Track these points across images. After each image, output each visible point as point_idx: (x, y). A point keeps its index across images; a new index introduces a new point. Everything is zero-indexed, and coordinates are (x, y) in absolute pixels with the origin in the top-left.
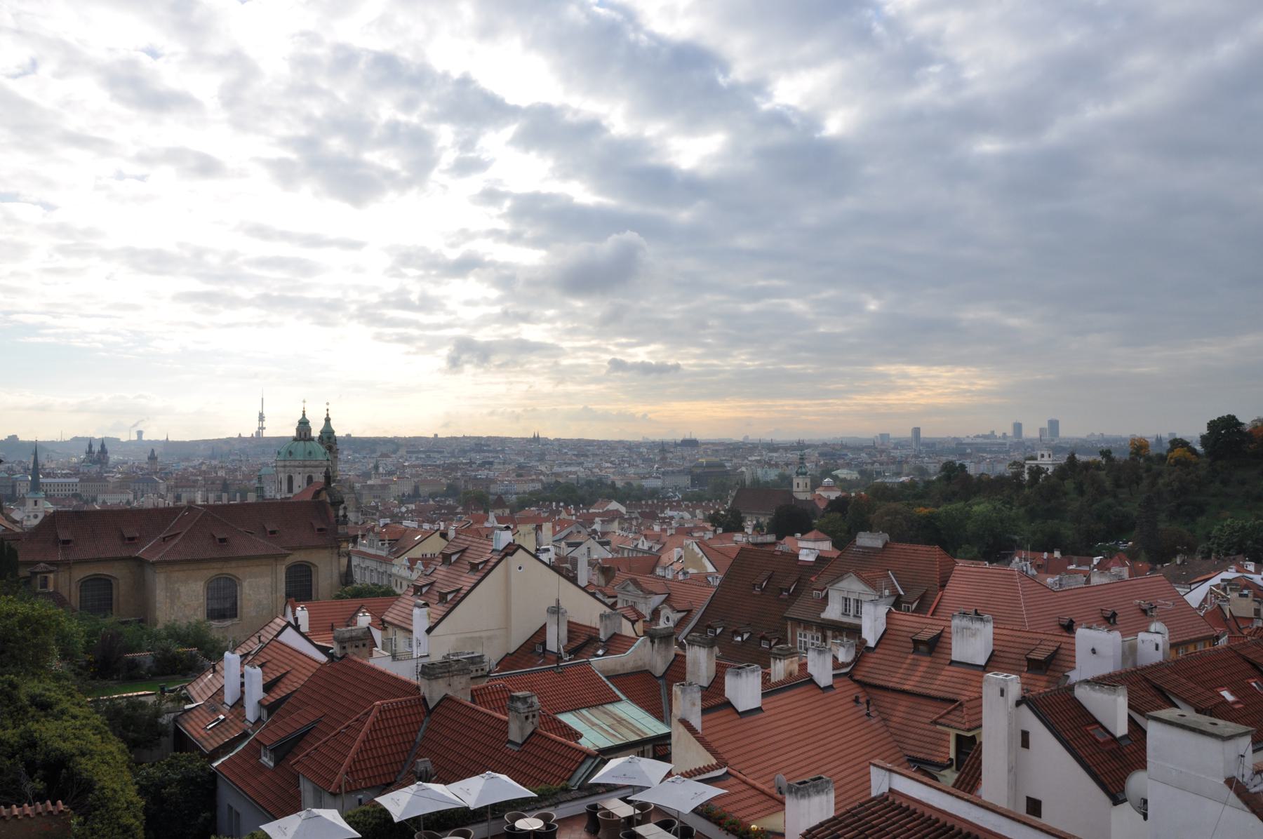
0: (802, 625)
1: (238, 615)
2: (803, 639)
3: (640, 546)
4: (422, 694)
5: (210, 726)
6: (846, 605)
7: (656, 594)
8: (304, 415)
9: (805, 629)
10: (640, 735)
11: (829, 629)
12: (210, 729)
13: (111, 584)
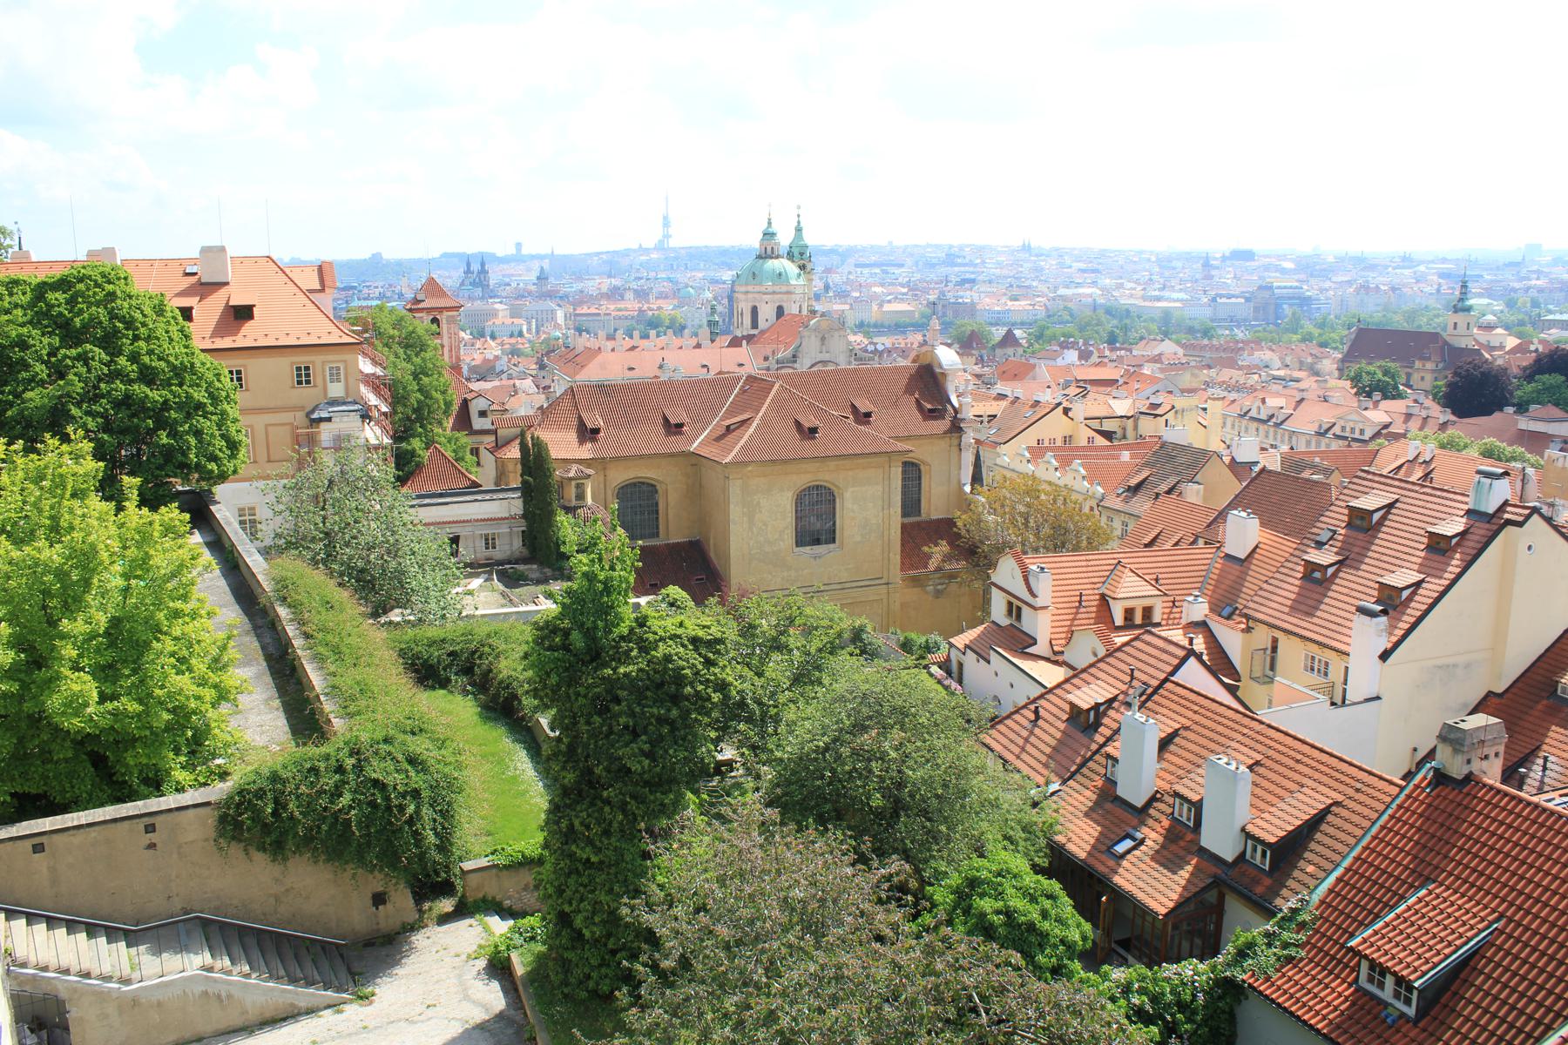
8: (770, 223)
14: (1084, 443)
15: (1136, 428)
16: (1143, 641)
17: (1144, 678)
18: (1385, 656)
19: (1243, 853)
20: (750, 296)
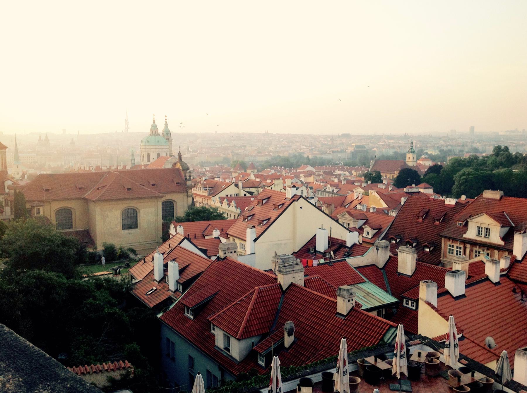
0: (451, 240)
1: (138, 227)
2: (451, 248)
3: (327, 190)
4: (278, 282)
5: (149, 293)
6: (479, 231)
7: (361, 220)
8: (154, 122)
10: (380, 303)
11: (468, 243)
12: (149, 295)
18: (255, 240)
19: (177, 289)
20: (147, 150)
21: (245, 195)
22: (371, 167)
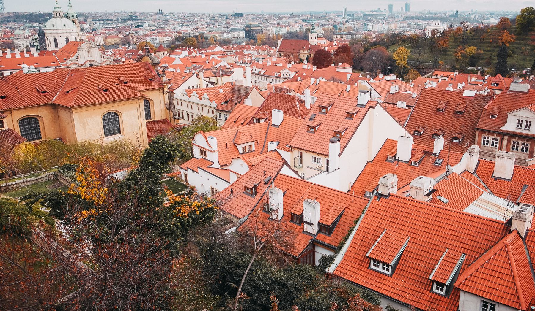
1: (121, 132)
2: (486, 140)
9: (488, 134)
13: (38, 120)
14: (204, 87)
15: (222, 80)
16: (266, 161)
17: (270, 174)
18: (340, 155)
21: (207, 86)
22: (279, 46)
